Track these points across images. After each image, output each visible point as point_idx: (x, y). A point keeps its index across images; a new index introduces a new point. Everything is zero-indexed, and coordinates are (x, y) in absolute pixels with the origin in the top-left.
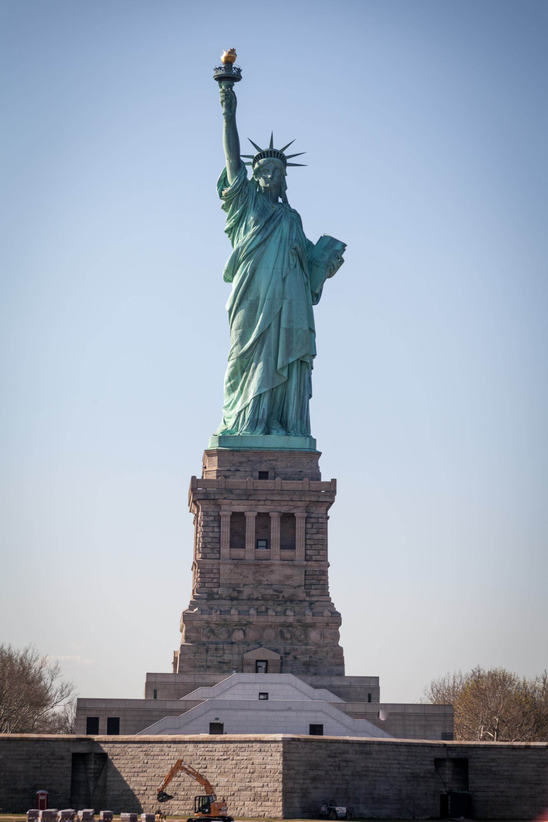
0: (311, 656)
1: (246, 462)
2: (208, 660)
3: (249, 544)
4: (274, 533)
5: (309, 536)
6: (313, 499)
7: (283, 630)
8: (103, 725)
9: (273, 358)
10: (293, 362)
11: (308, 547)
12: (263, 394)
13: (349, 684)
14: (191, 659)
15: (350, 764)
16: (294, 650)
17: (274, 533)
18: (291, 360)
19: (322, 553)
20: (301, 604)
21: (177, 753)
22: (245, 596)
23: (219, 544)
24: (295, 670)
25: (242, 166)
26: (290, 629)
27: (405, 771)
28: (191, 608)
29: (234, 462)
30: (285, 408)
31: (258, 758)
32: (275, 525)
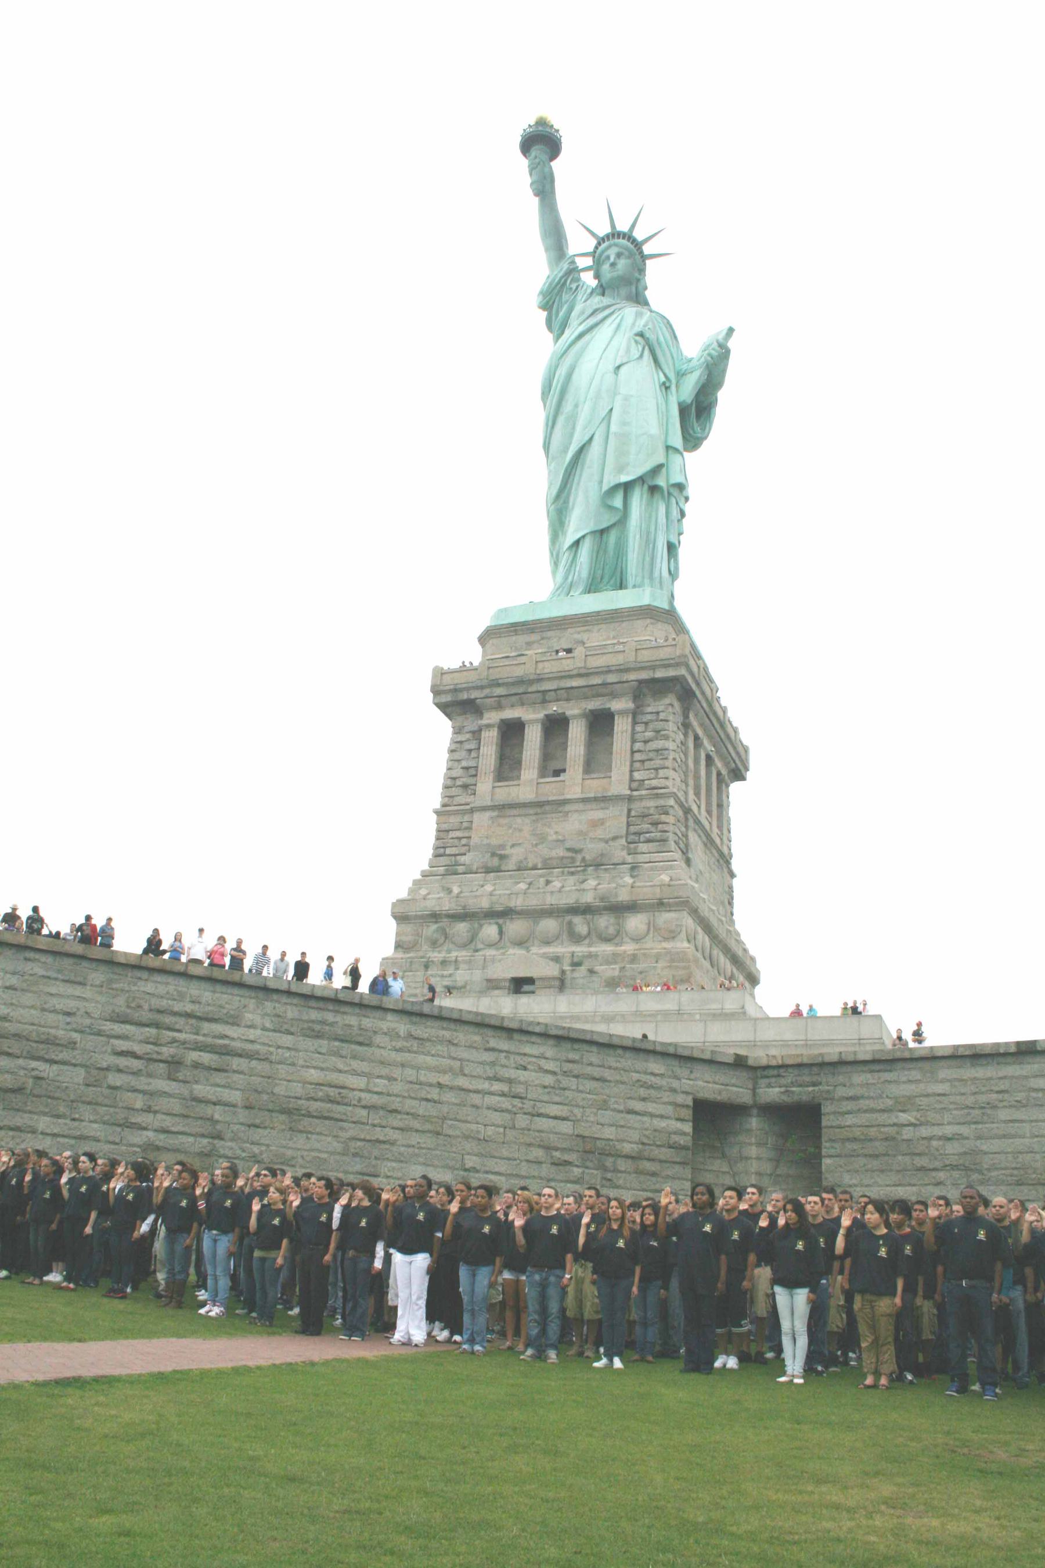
0: (624, 967)
1: (538, 642)
3: (527, 771)
4: (573, 747)
5: (638, 746)
6: (644, 675)
9: (596, 483)
11: (637, 765)
15: (236, 1063)
16: (590, 956)
17: (573, 747)
18: (624, 478)
19: (661, 773)
20: (614, 869)
22: (511, 864)
23: (475, 778)
28: (411, 891)
30: (624, 566)
32: (577, 733)
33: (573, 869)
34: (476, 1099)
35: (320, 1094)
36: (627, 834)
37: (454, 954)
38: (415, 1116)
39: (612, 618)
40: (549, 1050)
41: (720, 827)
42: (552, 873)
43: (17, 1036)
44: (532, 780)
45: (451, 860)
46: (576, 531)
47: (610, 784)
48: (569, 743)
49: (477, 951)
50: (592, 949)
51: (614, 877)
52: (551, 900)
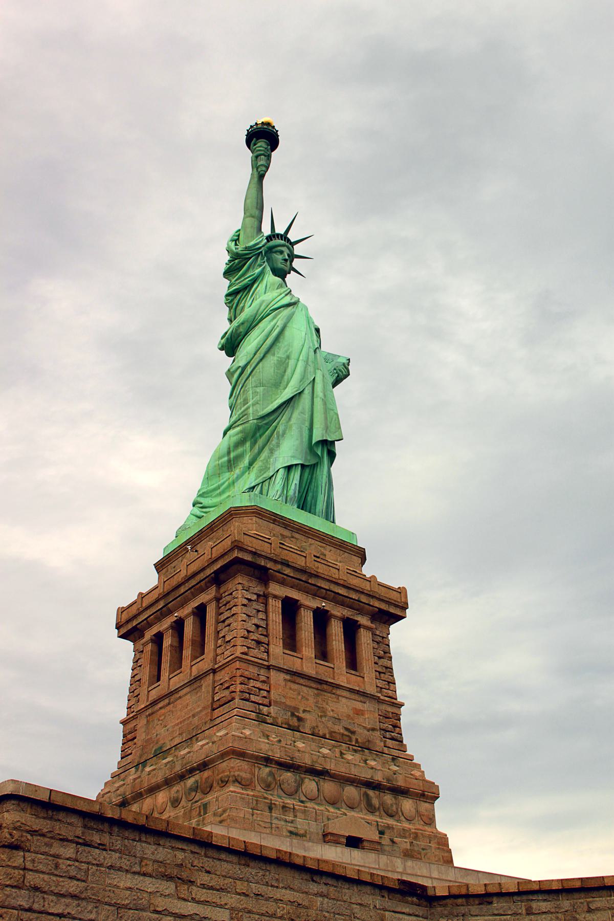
2: (274, 826)
4: (337, 642)
6: (383, 606)
7: (368, 792)
12: (294, 467)
16: (389, 827)
20: (382, 756)
23: (267, 639)
29: (274, 532)
30: (309, 498)
32: (336, 630)
36: (380, 729)
37: (289, 801)
39: (340, 546)
42: (341, 745)
44: (311, 658)
45: (255, 707)
47: (364, 682)
48: (334, 638)
51: (384, 763)
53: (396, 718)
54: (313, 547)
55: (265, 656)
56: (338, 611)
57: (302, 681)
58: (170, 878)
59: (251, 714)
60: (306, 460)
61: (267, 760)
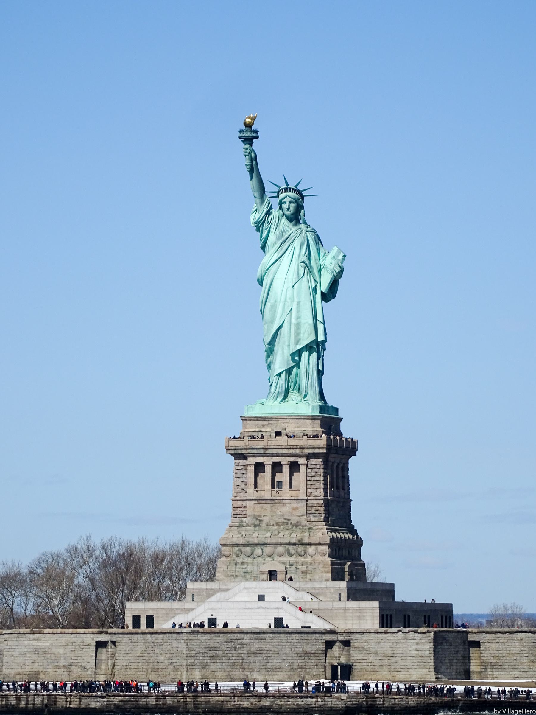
1: (267, 425)
2: (237, 571)
4: (284, 477)
5: (309, 478)
6: (311, 451)
8: (143, 621)
9: (287, 346)
10: (303, 348)
11: (309, 486)
13: (325, 587)
14: (225, 570)
15: (244, 646)
18: (299, 347)
19: (319, 490)
21: (143, 641)
24: (296, 577)
25: (266, 201)
26: (295, 547)
27: (296, 649)
29: (258, 425)
31: (175, 644)
33: (287, 528)
34: (284, 647)
35: (258, 650)
38: (274, 651)
39: (297, 418)
40: (297, 635)
41: (343, 489)
43: (212, 647)
44: (270, 489)
45: (240, 520)
46: (280, 368)
49: (254, 558)
50: (297, 560)
52: (280, 541)
53: (319, 506)
54: (278, 427)
55: (246, 495)
56: (284, 461)
57: (263, 502)
58: (36, 640)
59: (235, 524)
60: (288, 364)
61: (237, 545)
